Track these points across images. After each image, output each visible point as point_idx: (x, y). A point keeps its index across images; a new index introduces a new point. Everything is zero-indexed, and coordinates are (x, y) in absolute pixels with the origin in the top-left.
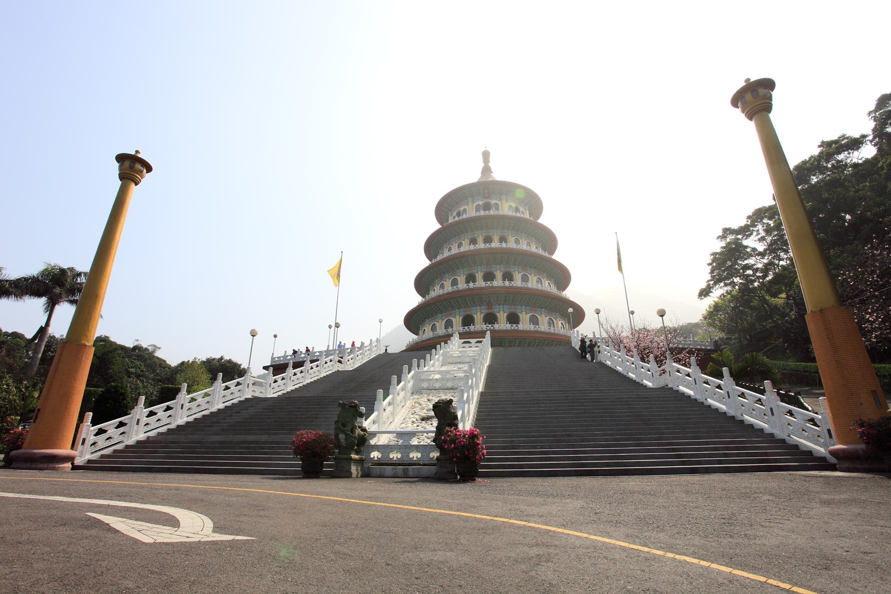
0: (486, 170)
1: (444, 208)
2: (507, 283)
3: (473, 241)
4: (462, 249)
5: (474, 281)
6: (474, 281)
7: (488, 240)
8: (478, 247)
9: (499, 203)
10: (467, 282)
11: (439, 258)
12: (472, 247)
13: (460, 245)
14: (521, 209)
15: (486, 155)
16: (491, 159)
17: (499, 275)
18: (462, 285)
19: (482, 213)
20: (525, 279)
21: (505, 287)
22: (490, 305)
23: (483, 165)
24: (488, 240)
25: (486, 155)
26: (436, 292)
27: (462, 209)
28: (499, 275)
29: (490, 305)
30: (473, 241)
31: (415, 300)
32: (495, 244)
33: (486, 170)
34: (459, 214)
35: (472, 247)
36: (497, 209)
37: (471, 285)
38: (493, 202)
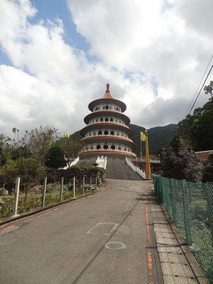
0: (108, 91)
1: (91, 106)
2: (112, 136)
3: (102, 120)
4: (98, 123)
5: (101, 134)
6: (101, 134)
7: (107, 120)
8: (103, 122)
9: (111, 106)
10: (99, 134)
11: (89, 124)
12: (101, 122)
13: (97, 121)
14: (119, 108)
15: (108, 86)
16: (110, 87)
17: (109, 119)
18: (97, 135)
19: (105, 110)
20: (118, 134)
21: (111, 137)
22: (106, 143)
23: (106, 89)
24: (107, 120)
25: (108, 86)
26: (91, 123)
27: (98, 107)
28: (109, 132)
29: (106, 143)
30: (102, 120)
31: (84, 125)
32: (109, 122)
33: (108, 91)
34: (97, 109)
35: (101, 122)
36: (110, 109)
37: (100, 135)
38: (109, 105)
